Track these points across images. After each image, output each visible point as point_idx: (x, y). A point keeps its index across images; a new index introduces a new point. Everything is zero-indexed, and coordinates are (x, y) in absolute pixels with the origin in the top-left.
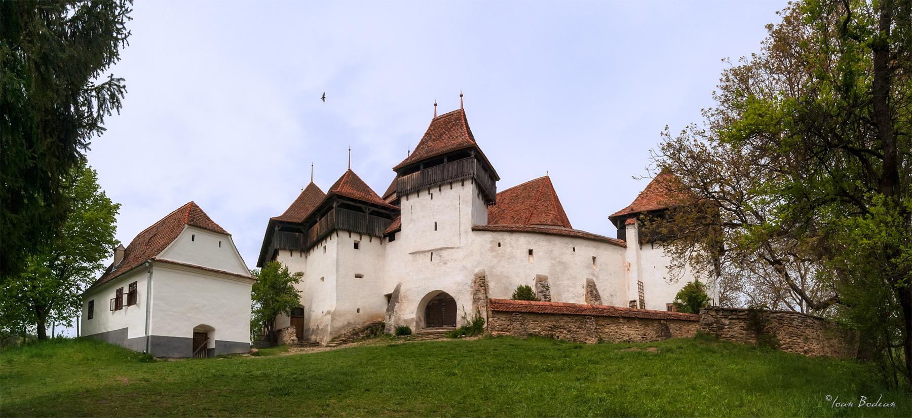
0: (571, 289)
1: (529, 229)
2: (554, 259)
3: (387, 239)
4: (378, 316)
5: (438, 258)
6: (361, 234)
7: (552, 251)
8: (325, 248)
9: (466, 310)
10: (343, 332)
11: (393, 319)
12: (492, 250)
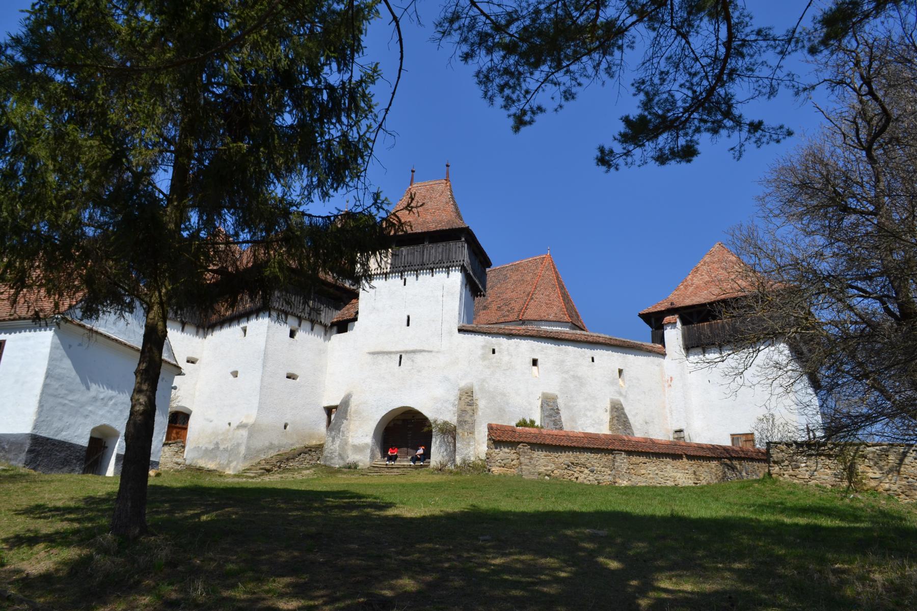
0: (589, 414)
1: (534, 333)
2: (567, 372)
3: (335, 329)
4: (311, 437)
6: (300, 319)
7: (563, 361)
10: (263, 457)
11: (338, 442)
12: (484, 357)
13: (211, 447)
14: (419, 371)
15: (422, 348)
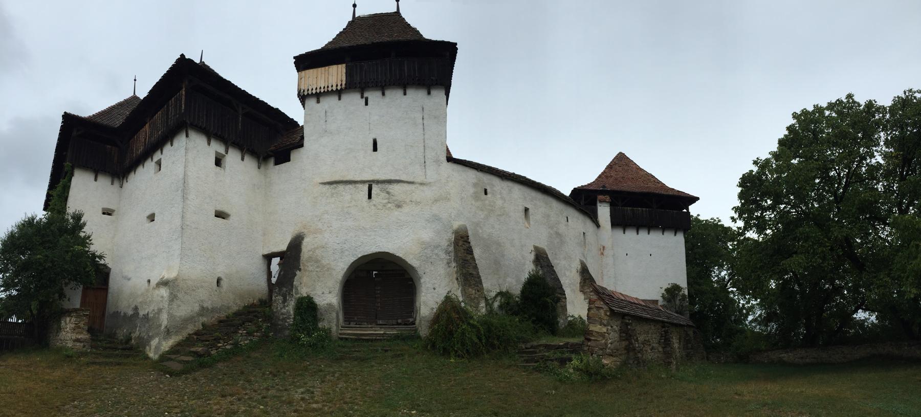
3: (272, 161)
5: (384, 195)
8: (159, 163)
9: (435, 289)
13: (130, 312)
14: (399, 206)
15: (398, 178)
